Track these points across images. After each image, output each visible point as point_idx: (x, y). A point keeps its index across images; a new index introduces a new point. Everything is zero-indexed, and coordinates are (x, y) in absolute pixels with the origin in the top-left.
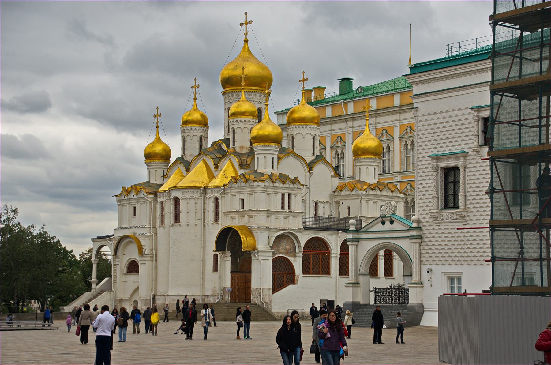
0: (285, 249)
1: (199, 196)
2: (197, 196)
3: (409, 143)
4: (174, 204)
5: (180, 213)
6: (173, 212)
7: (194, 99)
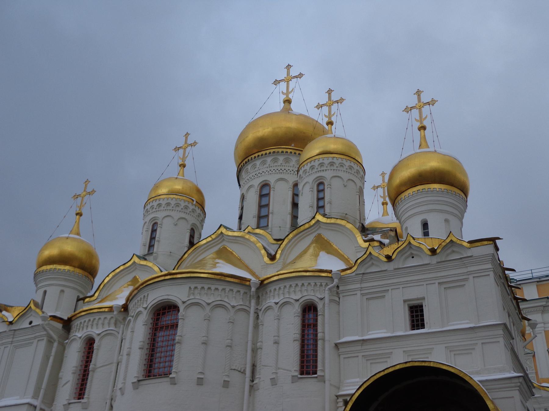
1: (242, 303)
2: (234, 303)
4: (150, 326)
5: (173, 345)
6: (147, 346)
7: (180, 166)
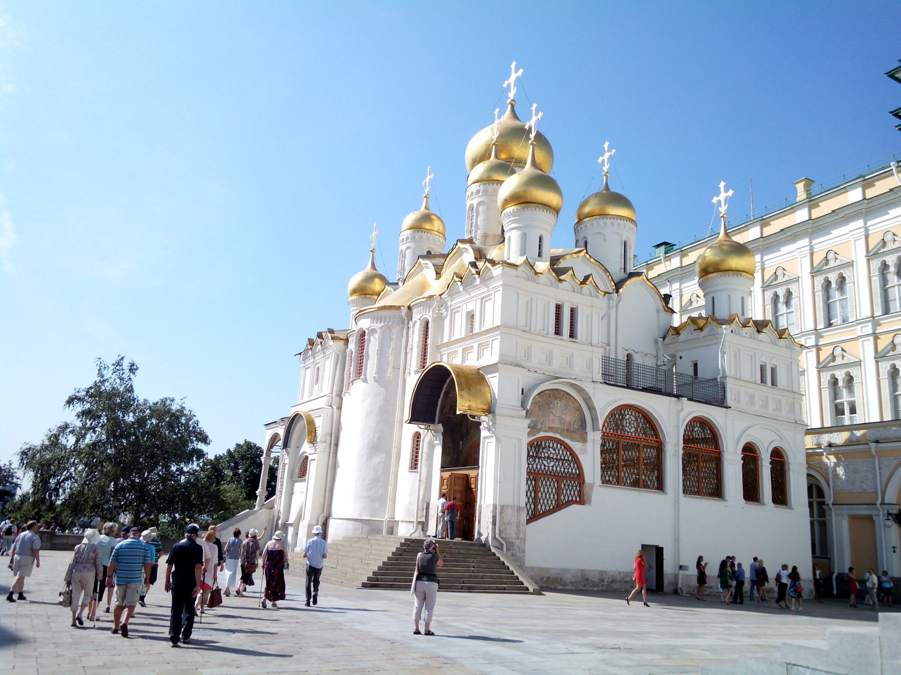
0: (561, 420)
3: (781, 292)
